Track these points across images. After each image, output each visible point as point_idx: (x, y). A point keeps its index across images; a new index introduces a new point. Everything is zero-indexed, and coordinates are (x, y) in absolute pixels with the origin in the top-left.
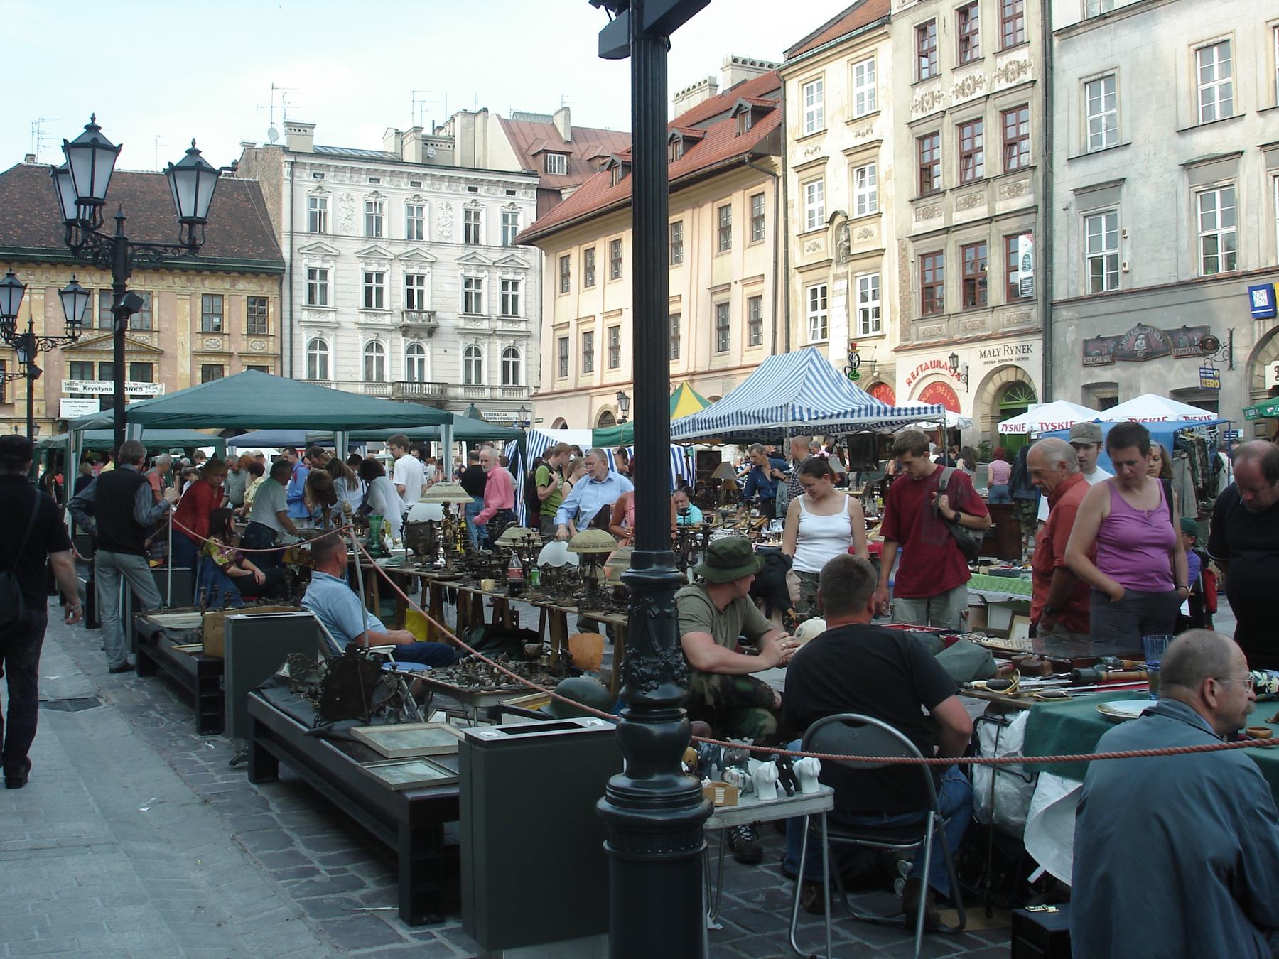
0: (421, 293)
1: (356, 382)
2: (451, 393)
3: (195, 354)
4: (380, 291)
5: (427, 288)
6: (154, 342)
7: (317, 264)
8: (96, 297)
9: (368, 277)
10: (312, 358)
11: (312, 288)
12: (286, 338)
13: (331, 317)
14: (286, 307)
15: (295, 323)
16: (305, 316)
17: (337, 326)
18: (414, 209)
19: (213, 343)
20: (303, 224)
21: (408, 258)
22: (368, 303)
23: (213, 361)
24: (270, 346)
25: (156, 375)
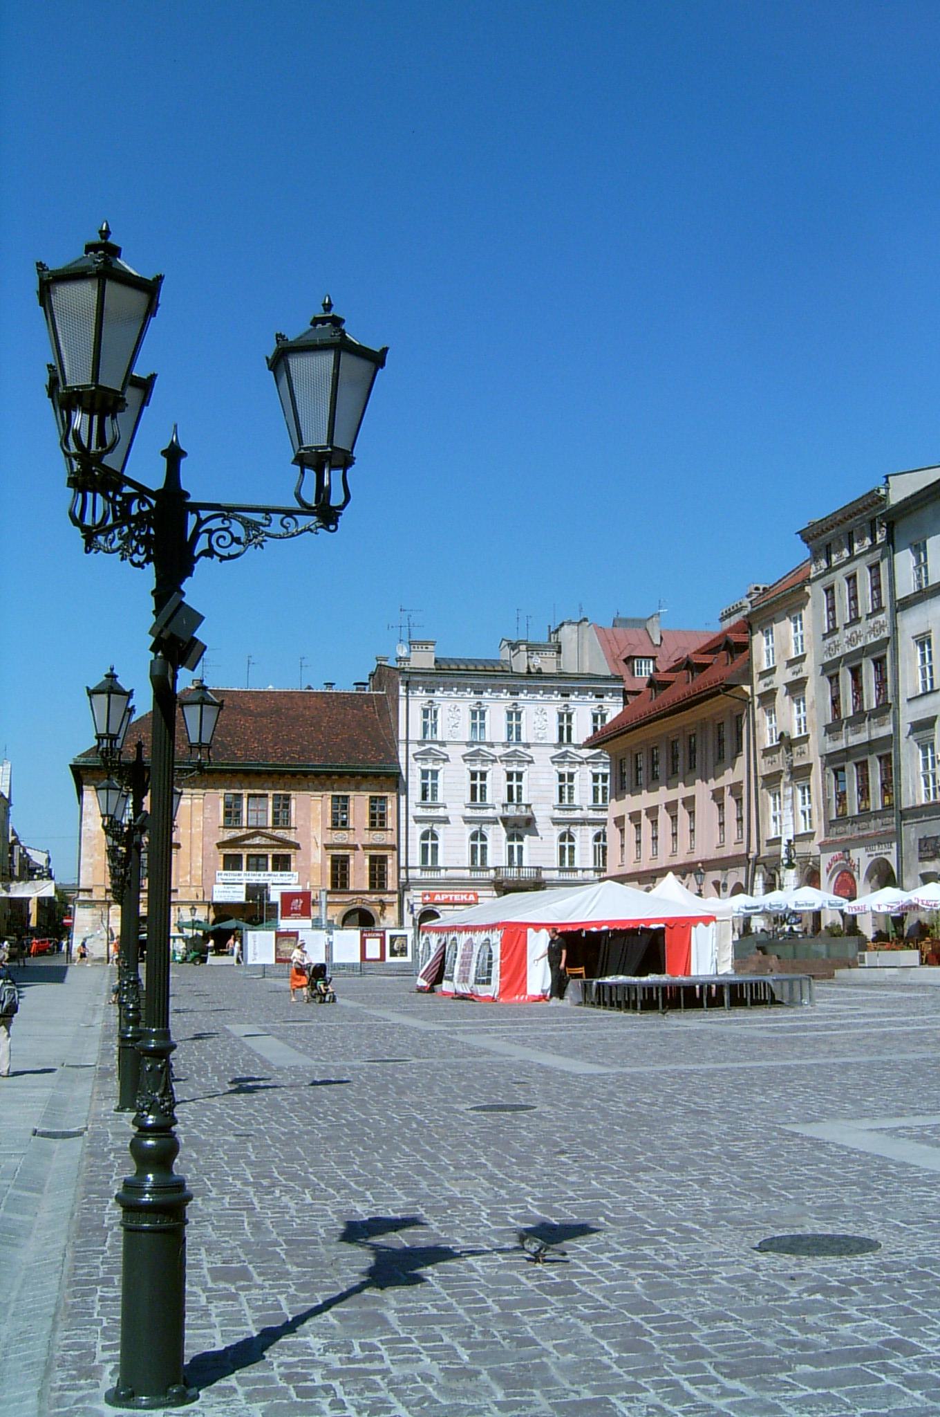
0: (519, 787)
1: (465, 868)
2: (545, 875)
3: (327, 847)
4: (483, 787)
5: (524, 783)
6: (291, 836)
7: (430, 766)
8: (245, 800)
9: (474, 776)
10: (425, 847)
11: (424, 786)
12: (403, 830)
13: (441, 812)
14: (403, 804)
15: (411, 818)
16: (420, 812)
17: (445, 821)
18: (514, 714)
19: (340, 837)
20: (416, 734)
21: (508, 758)
22: (473, 798)
23: (341, 852)
24: (388, 838)
25: (293, 864)
